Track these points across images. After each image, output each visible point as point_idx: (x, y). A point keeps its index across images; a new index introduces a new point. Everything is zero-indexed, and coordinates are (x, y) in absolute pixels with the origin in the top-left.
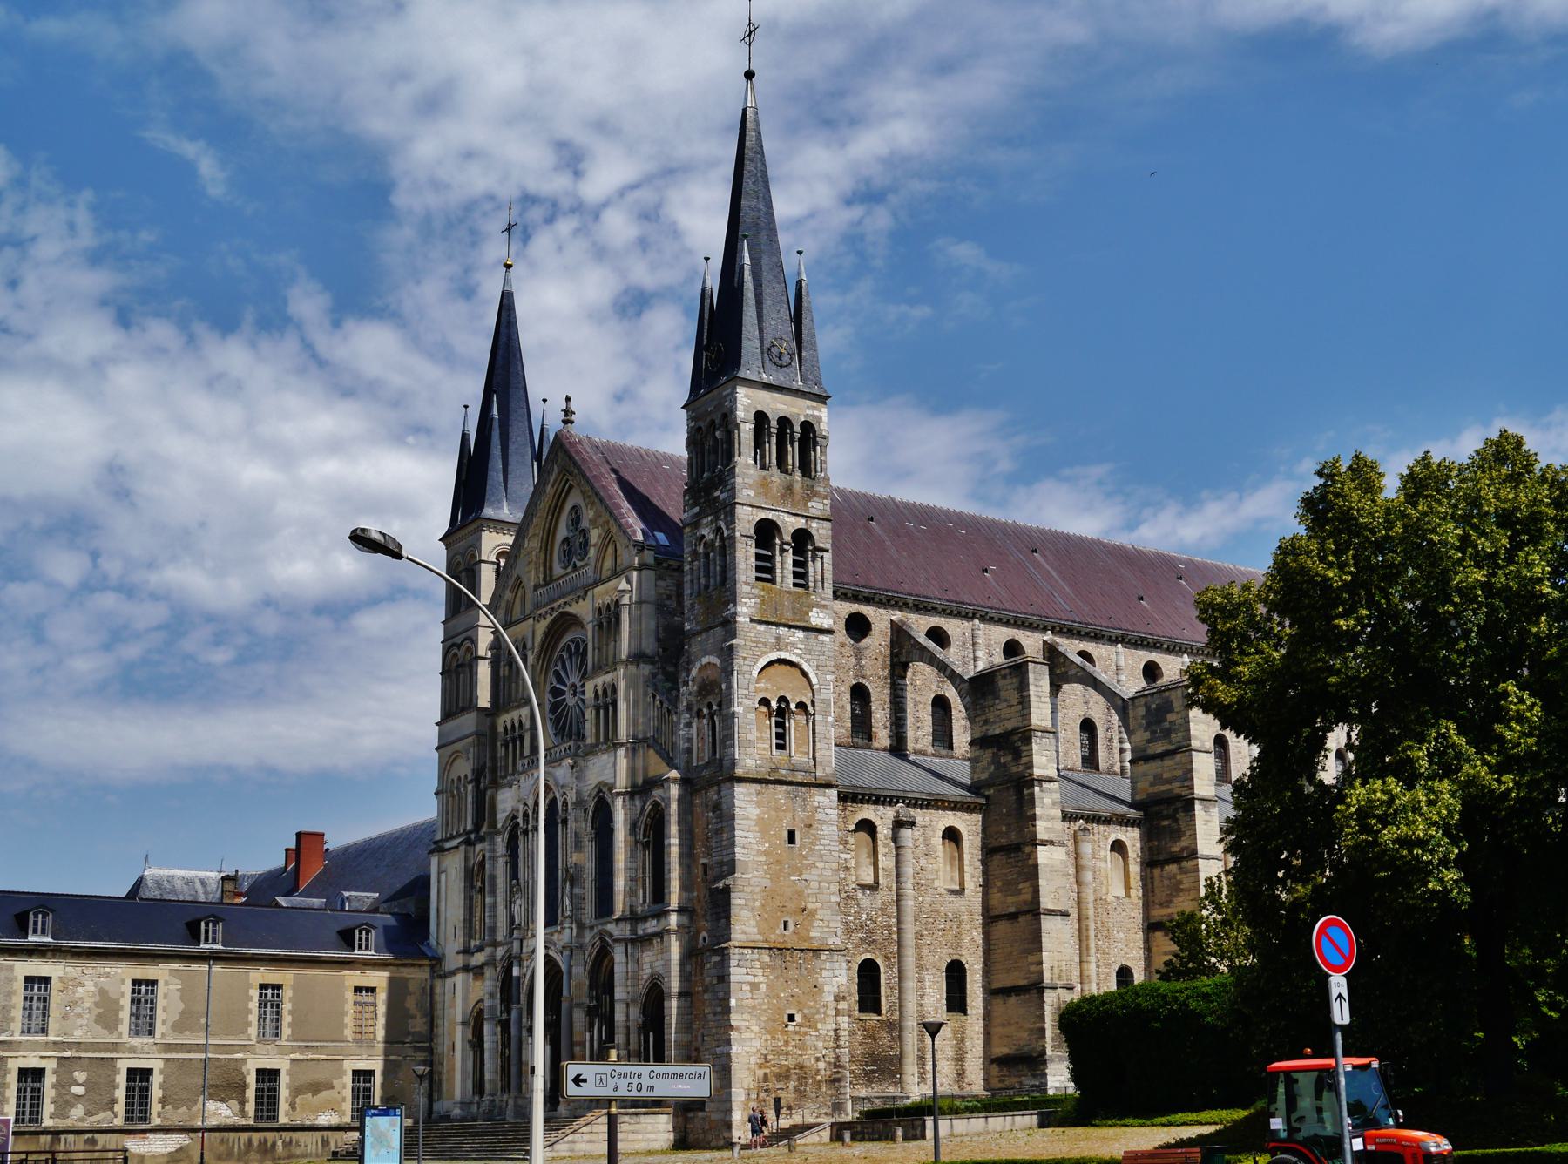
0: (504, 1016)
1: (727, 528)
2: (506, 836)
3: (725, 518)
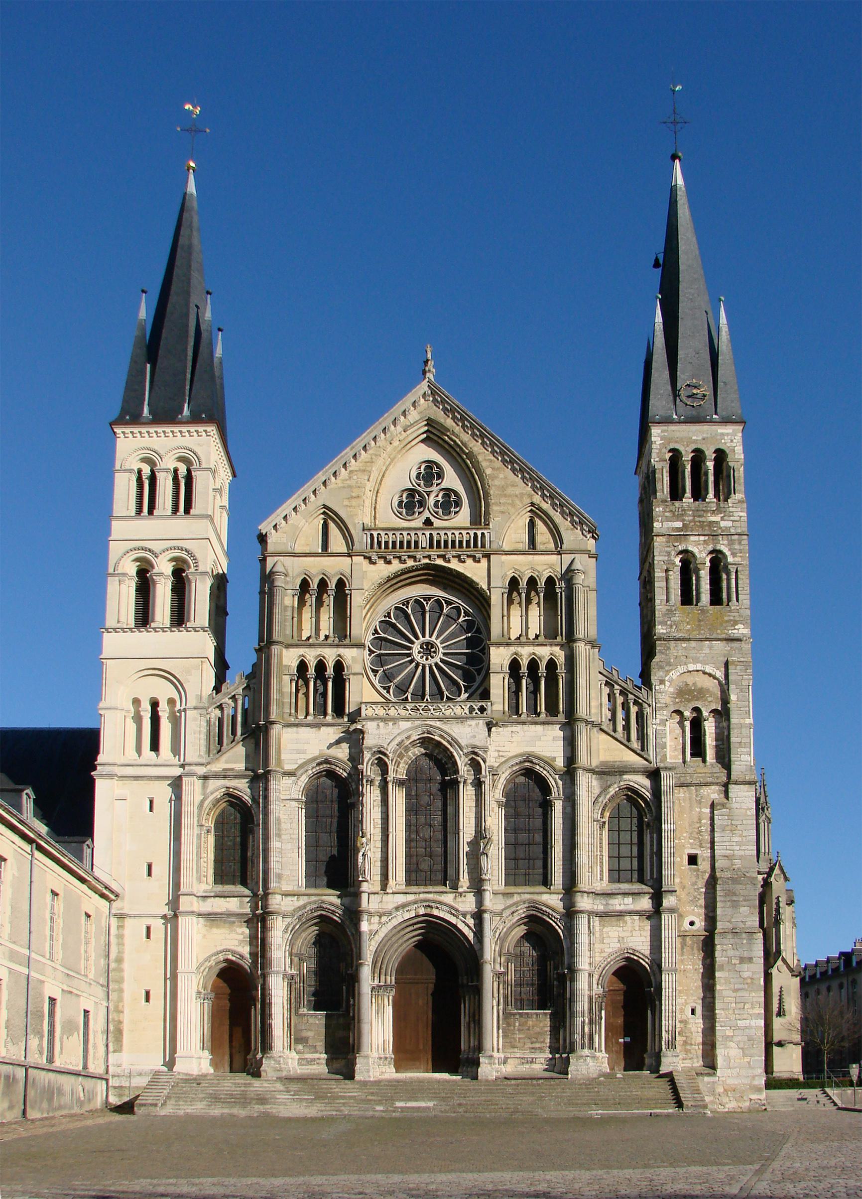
0: (294, 972)
1: (734, 555)
2: (304, 779)
3: (729, 545)
